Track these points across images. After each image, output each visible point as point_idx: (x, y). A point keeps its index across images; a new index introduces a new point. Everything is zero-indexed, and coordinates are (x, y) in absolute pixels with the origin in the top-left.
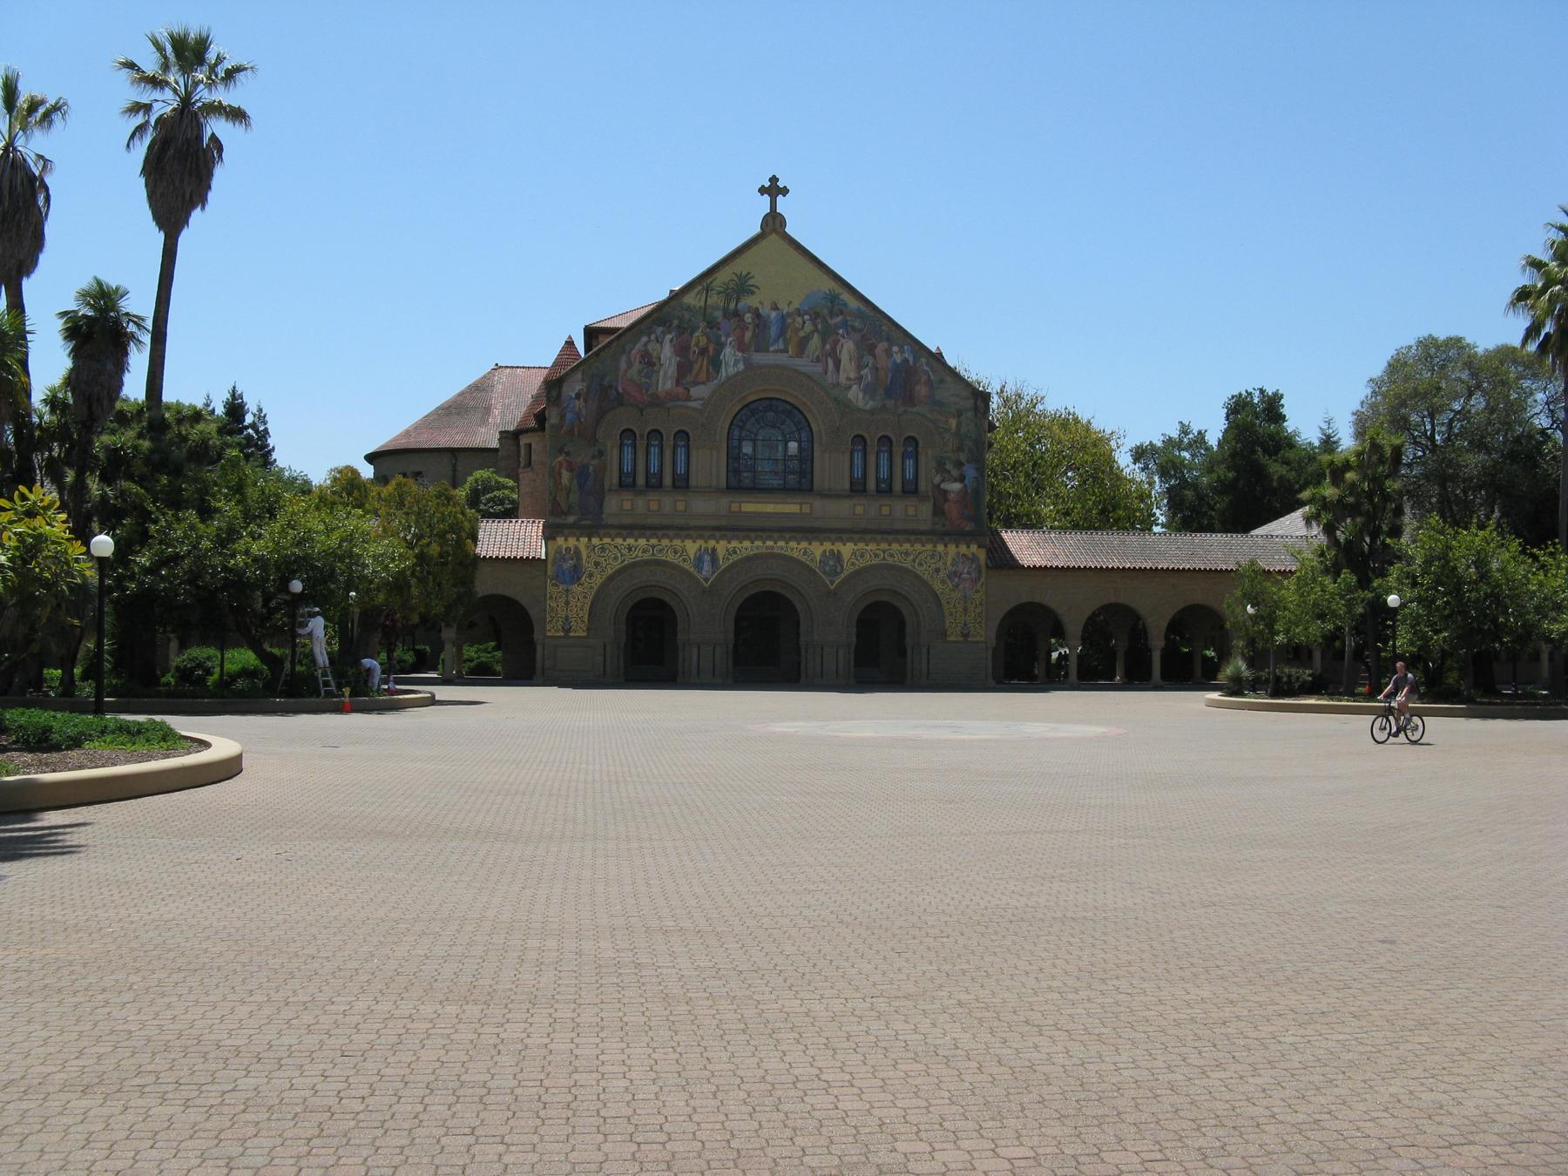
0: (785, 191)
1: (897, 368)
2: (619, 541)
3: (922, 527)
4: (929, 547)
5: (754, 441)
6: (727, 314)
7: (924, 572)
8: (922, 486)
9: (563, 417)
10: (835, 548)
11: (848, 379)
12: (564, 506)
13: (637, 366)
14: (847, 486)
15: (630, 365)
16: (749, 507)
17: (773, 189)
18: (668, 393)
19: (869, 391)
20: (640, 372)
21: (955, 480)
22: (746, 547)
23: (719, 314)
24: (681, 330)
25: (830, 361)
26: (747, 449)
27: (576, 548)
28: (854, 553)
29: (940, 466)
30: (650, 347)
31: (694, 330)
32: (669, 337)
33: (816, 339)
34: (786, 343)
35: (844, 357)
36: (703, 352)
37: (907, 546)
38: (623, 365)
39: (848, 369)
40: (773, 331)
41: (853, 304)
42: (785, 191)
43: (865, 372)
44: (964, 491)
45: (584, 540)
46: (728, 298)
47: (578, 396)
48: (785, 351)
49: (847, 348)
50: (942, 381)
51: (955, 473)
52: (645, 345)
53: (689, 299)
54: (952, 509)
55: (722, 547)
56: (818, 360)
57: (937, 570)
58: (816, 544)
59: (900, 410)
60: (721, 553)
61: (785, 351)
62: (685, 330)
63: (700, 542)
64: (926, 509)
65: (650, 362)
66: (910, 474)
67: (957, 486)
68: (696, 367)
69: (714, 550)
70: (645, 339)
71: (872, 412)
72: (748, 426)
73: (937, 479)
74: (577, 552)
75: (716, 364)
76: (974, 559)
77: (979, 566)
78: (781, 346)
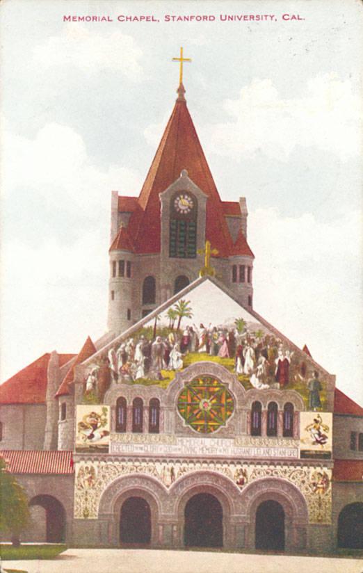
2: (116, 463)
4: (299, 468)
7: (295, 483)
25: (239, 360)
27: (92, 467)
28: (254, 472)
55: (177, 467)
57: (303, 482)
58: (232, 466)
60: (176, 472)
63: (164, 464)
69: (172, 469)
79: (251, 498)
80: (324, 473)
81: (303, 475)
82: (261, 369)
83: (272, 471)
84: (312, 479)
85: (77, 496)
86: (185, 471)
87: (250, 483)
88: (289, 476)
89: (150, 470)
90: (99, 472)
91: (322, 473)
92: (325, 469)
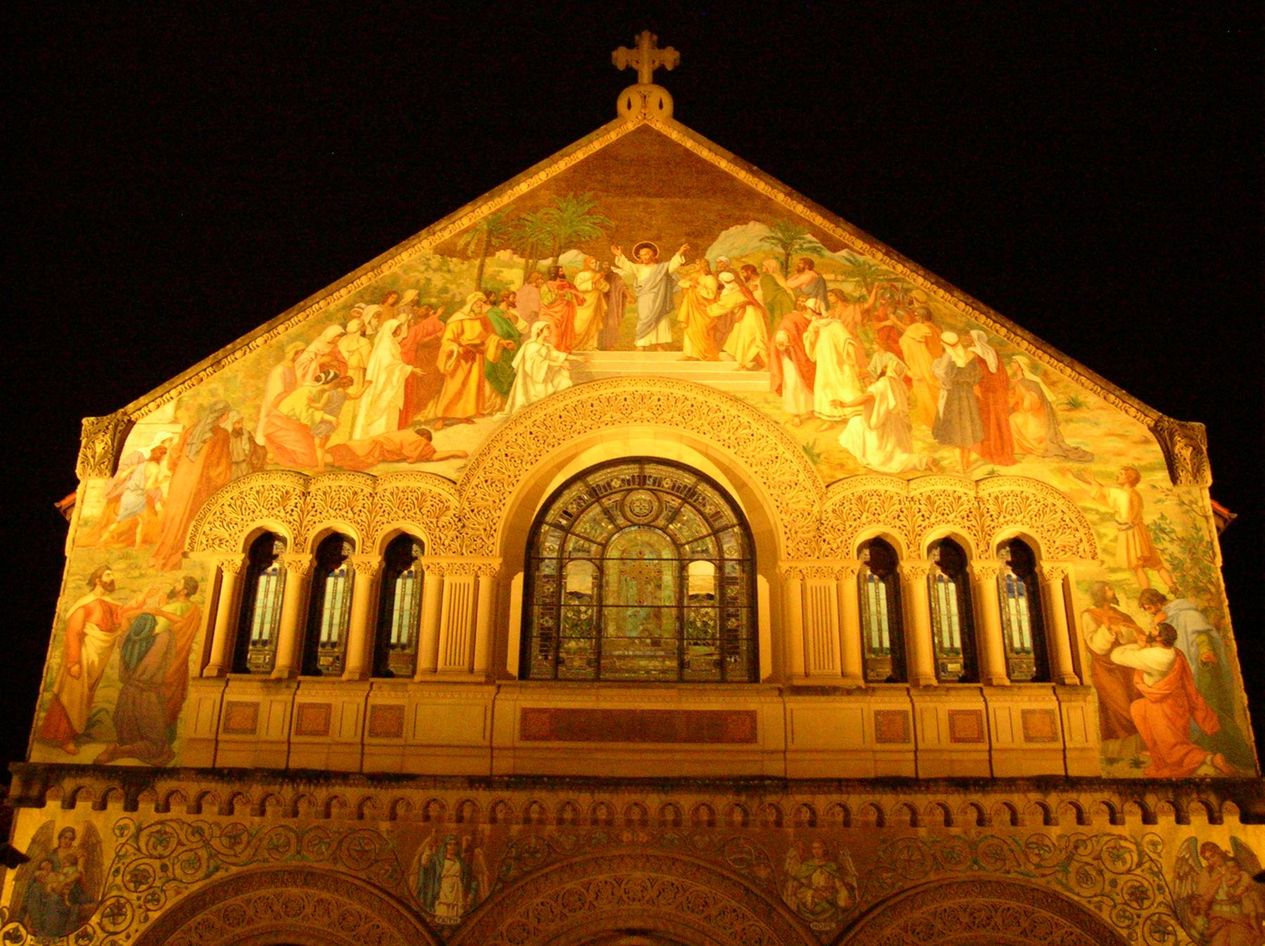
1: (956, 376)
9: (114, 500)
12: (76, 718)
13: (308, 387)
14: (855, 666)
18: (376, 443)
19: (895, 427)
20: (312, 400)
21: (1151, 640)
25: (789, 368)
26: (579, 579)
27: (91, 831)
30: (343, 346)
31: (451, 307)
32: (393, 323)
36: (471, 353)
39: (835, 381)
40: (646, 305)
43: (877, 388)
45: (115, 809)
48: (676, 346)
50: (1074, 405)
51: (1146, 621)
52: (334, 342)
54: (1152, 717)
56: (758, 363)
59: (979, 473)
64: (1082, 717)
66: (1023, 637)
67: (1157, 657)
68: (452, 387)
70: (334, 330)
71: (907, 477)
72: (579, 529)
73: (1100, 640)
74: (91, 845)
75: (501, 378)
78: (664, 334)
91: (1225, 846)
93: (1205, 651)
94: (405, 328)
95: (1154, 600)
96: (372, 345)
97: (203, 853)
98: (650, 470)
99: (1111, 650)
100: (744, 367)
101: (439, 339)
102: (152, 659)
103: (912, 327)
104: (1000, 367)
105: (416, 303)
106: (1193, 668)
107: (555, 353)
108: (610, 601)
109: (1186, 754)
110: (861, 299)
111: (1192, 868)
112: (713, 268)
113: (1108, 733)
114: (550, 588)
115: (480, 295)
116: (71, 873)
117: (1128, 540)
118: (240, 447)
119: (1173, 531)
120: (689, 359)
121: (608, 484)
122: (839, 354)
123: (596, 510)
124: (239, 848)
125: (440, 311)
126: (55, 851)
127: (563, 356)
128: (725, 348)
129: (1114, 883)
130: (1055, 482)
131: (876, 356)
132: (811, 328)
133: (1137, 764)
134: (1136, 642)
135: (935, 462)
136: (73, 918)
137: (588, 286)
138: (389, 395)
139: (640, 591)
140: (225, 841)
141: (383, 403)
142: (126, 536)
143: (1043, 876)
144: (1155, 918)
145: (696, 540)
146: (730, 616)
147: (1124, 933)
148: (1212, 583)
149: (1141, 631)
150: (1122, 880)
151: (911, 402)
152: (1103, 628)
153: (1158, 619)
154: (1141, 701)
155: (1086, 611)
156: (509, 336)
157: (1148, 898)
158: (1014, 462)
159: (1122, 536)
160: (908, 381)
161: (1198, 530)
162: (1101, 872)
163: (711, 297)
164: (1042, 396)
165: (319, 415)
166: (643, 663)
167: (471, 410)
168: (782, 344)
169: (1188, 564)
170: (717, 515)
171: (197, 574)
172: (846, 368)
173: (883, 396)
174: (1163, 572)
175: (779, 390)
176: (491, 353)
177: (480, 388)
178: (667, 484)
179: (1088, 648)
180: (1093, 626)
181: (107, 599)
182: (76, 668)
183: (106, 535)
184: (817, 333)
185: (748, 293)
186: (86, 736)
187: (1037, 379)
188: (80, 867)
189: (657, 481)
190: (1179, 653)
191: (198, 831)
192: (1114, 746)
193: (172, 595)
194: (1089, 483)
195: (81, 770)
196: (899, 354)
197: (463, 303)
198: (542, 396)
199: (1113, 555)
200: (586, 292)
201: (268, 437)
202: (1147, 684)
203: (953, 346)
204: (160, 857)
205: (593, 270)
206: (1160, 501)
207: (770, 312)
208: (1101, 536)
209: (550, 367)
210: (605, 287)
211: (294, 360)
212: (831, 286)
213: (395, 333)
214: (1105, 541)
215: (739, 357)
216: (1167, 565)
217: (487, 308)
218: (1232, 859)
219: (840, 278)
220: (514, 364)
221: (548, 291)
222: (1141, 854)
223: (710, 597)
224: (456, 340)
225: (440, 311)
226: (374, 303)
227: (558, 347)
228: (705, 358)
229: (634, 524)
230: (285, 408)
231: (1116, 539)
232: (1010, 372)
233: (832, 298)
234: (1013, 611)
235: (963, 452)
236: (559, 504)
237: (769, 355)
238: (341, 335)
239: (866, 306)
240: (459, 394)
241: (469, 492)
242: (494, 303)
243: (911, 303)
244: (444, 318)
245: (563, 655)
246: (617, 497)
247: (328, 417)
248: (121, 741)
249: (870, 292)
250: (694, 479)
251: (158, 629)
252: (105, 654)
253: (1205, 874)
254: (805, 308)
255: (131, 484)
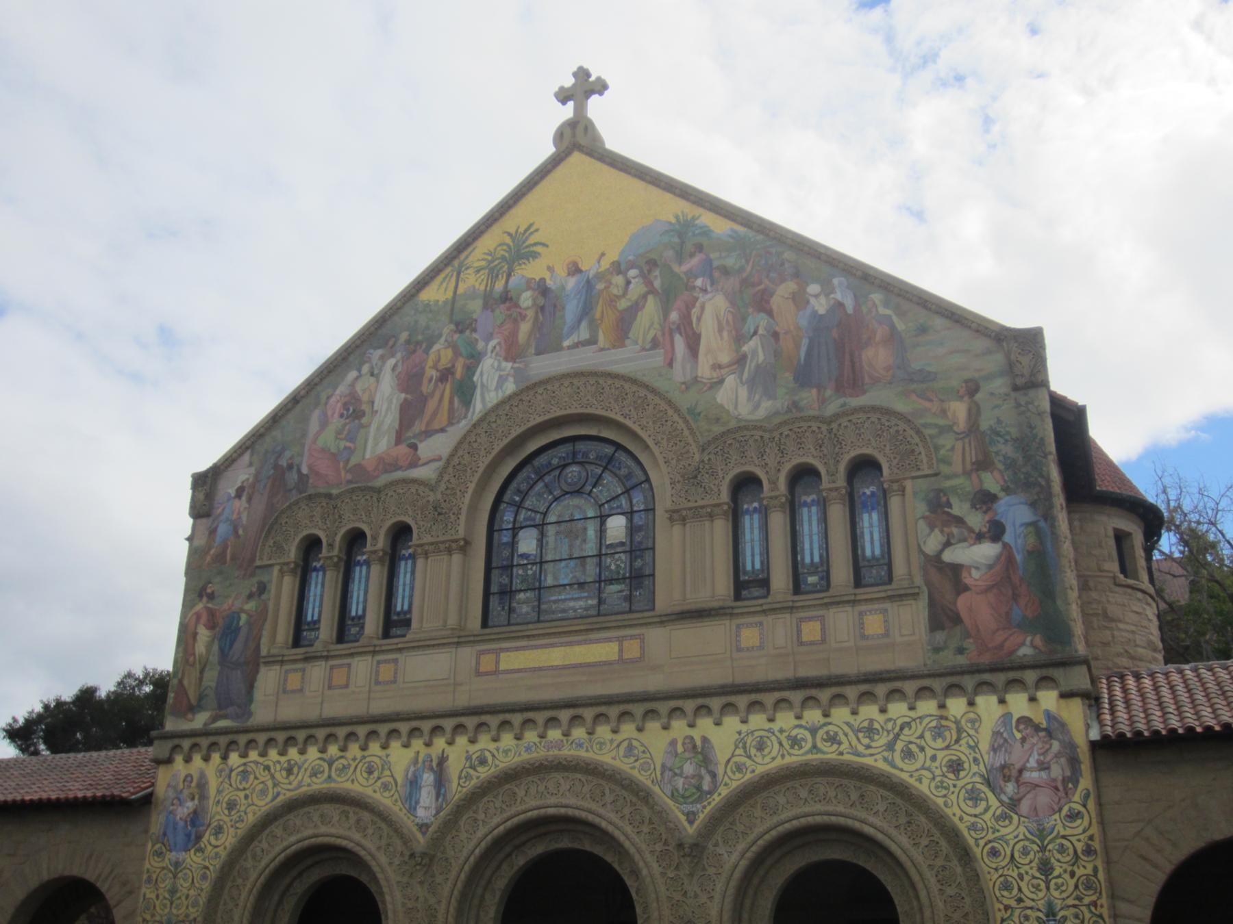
0: (600, 87)
3: (902, 662)
4: (928, 707)
5: (541, 527)
6: (489, 302)
8: (899, 568)
10: (696, 734)
11: (717, 367)
13: (336, 422)
14: (722, 586)
15: (324, 424)
16: (514, 659)
17: (584, 87)
18: (380, 459)
19: (763, 380)
20: (338, 433)
21: (980, 538)
22: (507, 750)
23: (476, 306)
24: (412, 346)
26: (527, 543)
27: (202, 775)
28: (741, 743)
29: (938, 508)
30: (359, 387)
32: (392, 361)
33: (651, 305)
34: (593, 327)
35: (707, 327)
37: (870, 711)
38: (314, 426)
40: (571, 310)
41: (720, 227)
42: (600, 87)
44: (1007, 558)
46: (493, 274)
47: (240, 492)
48: (592, 341)
49: (713, 309)
50: (923, 330)
51: (976, 520)
52: (352, 385)
53: (431, 294)
54: (977, 608)
55: (458, 752)
56: (655, 344)
57: (956, 767)
59: (832, 408)
61: (592, 341)
62: (419, 344)
65: (355, 411)
67: (986, 551)
68: (432, 405)
69: (442, 760)
70: (353, 374)
72: (527, 504)
73: (932, 543)
74: (202, 785)
75: (465, 391)
76: (1052, 728)
77: (1071, 746)
78: (584, 334)
79: (733, 856)
80: (1048, 715)
81: (950, 736)
82: (755, 352)
83: (813, 731)
84: (994, 749)
85: (149, 880)
86: (483, 762)
87: (724, 791)
88: (890, 747)
89: (370, 772)
90: (219, 792)
92: (1049, 699)
93: (1032, 540)
94: (400, 364)
95: (985, 500)
96: (378, 381)
97: (270, 783)
98: (581, 446)
99: (942, 551)
100: (644, 349)
101: (423, 369)
102: (238, 645)
103: (783, 286)
104: (857, 308)
105: (408, 342)
106: (1019, 558)
107: (504, 364)
108: (549, 558)
109: (1007, 639)
110: (742, 269)
111: (1006, 740)
112: (623, 267)
113: (935, 624)
114: (506, 553)
115: (452, 327)
116: (190, 805)
117: (964, 449)
118: (292, 477)
119: (1008, 433)
120: (602, 350)
121: (550, 463)
122: (719, 323)
123: (540, 485)
124: (292, 778)
125: (424, 346)
126: (181, 791)
127: (509, 365)
128: (631, 335)
129: (934, 758)
130: (901, 406)
131: (750, 320)
132: (698, 304)
133: (961, 651)
134: (965, 540)
135: (795, 404)
136: (193, 837)
137: (529, 303)
138: (388, 420)
139: (571, 546)
140: (284, 773)
141: (385, 427)
142: (220, 558)
143: (872, 755)
144: (969, 787)
145: (613, 499)
146: (636, 558)
147: (940, 801)
148: (1042, 476)
149: (971, 530)
150: (940, 755)
151: (777, 354)
152: (937, 531)
153: (987, 518)
154: (967, 593)
155: (924, 517)
156: (472, 356)
157: (964, 770)
158: (864, 392)
159: (959, 445)
160: (776, 335)
161: (1031, 427)
162: (922, 749)
163: (621, 293)
164: (893, 327)
165: (343, 444)
166: (572, 604)
167: (445, 423)
168: (674, 323)
169: (1021, 461)
170: (629, 476)
171: (265, 579)
172: (725, 334)
173: (755, 352)
174: (996, 473)
175: (670, 364)
176: (459, 371)
177: (451, 402)
178: (592, 456)
179: (921, 551)
180: (927, 530)
181: (210, 605)
182: (191, 659)
183: (208, 559)
184: (703, 308)
185: (649, 283)
186: (193, 709)
187: (888, 312)
188: (196, 802)
189: (585, 454)
190: (1006, 546)
191: (267, 768)
192: (940, 636)
193: (250, 596)
194: (931, 401)
195: (193, 734)
196: (770, 313)
197: (440, 336)
198: (495, 402)
199: (950, 464)
200: (527, 308)
201: (310, 467)
202: (974, 578)
203: (816, 296)
204: (245, 789)
205: (533, 290)
206: (997, 406)
207: (667, 298)
208: (937, 448)
209: (500, 376)
210: (541, 301)
211: (326, 404)
212: (715, 264)
213: (394, 369)
214: (942, 452)
215: (640, 342)
216: (1001, 467)
217: (456, 336)
218: (1045, 730)
219: (724, 254)
220: (475, 379)
221: (500, 312)
222: (960, 730)
223: (622, 544)
224: (435, 367)
225: (424, 346)
226: (379, 348)
227: (506, 359)
228: (614, 347)
229: (567, 493)
230: (320, 443)
231: (953, 449)
232: (864, 309)
233: (716, 274)
234: (866, 524)
235: (819, 391)
236: (514, 485)
237: (663, 334)
238: (357, 378)
239: (744, 275)
240: (435, 414)
241: (443, 486)
242: (461, 332)
243: (782, 264)
244: (427, 351)
245: (514, 605)
246: (557, 472)
247: (348, 444)
248: (220, 707)
249: (747, 261)
250: (613, 449)
251: (242, 623)
252: (209, 647)
253: (1018, 745)
254: (694, 287)
255: (223, 517)
